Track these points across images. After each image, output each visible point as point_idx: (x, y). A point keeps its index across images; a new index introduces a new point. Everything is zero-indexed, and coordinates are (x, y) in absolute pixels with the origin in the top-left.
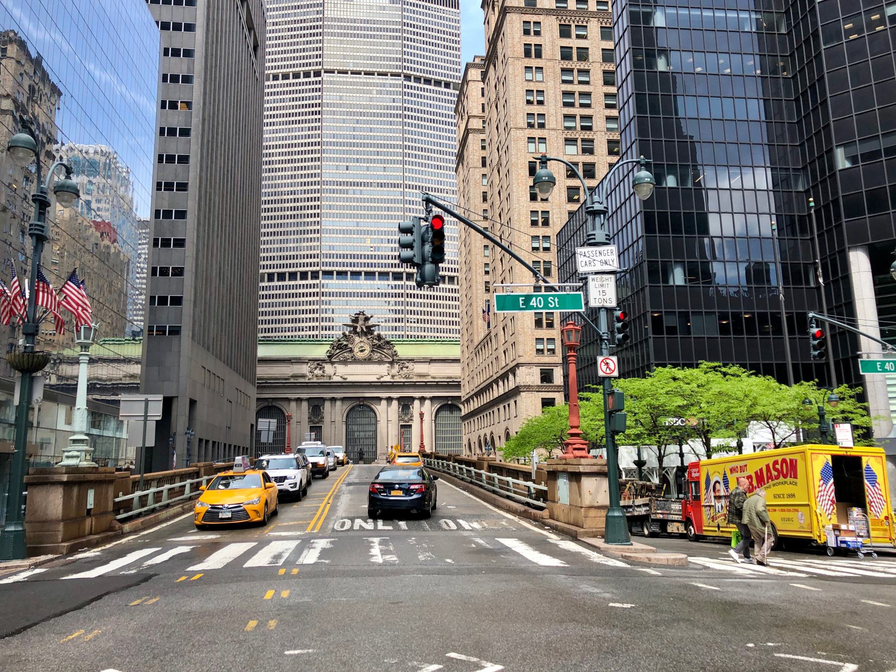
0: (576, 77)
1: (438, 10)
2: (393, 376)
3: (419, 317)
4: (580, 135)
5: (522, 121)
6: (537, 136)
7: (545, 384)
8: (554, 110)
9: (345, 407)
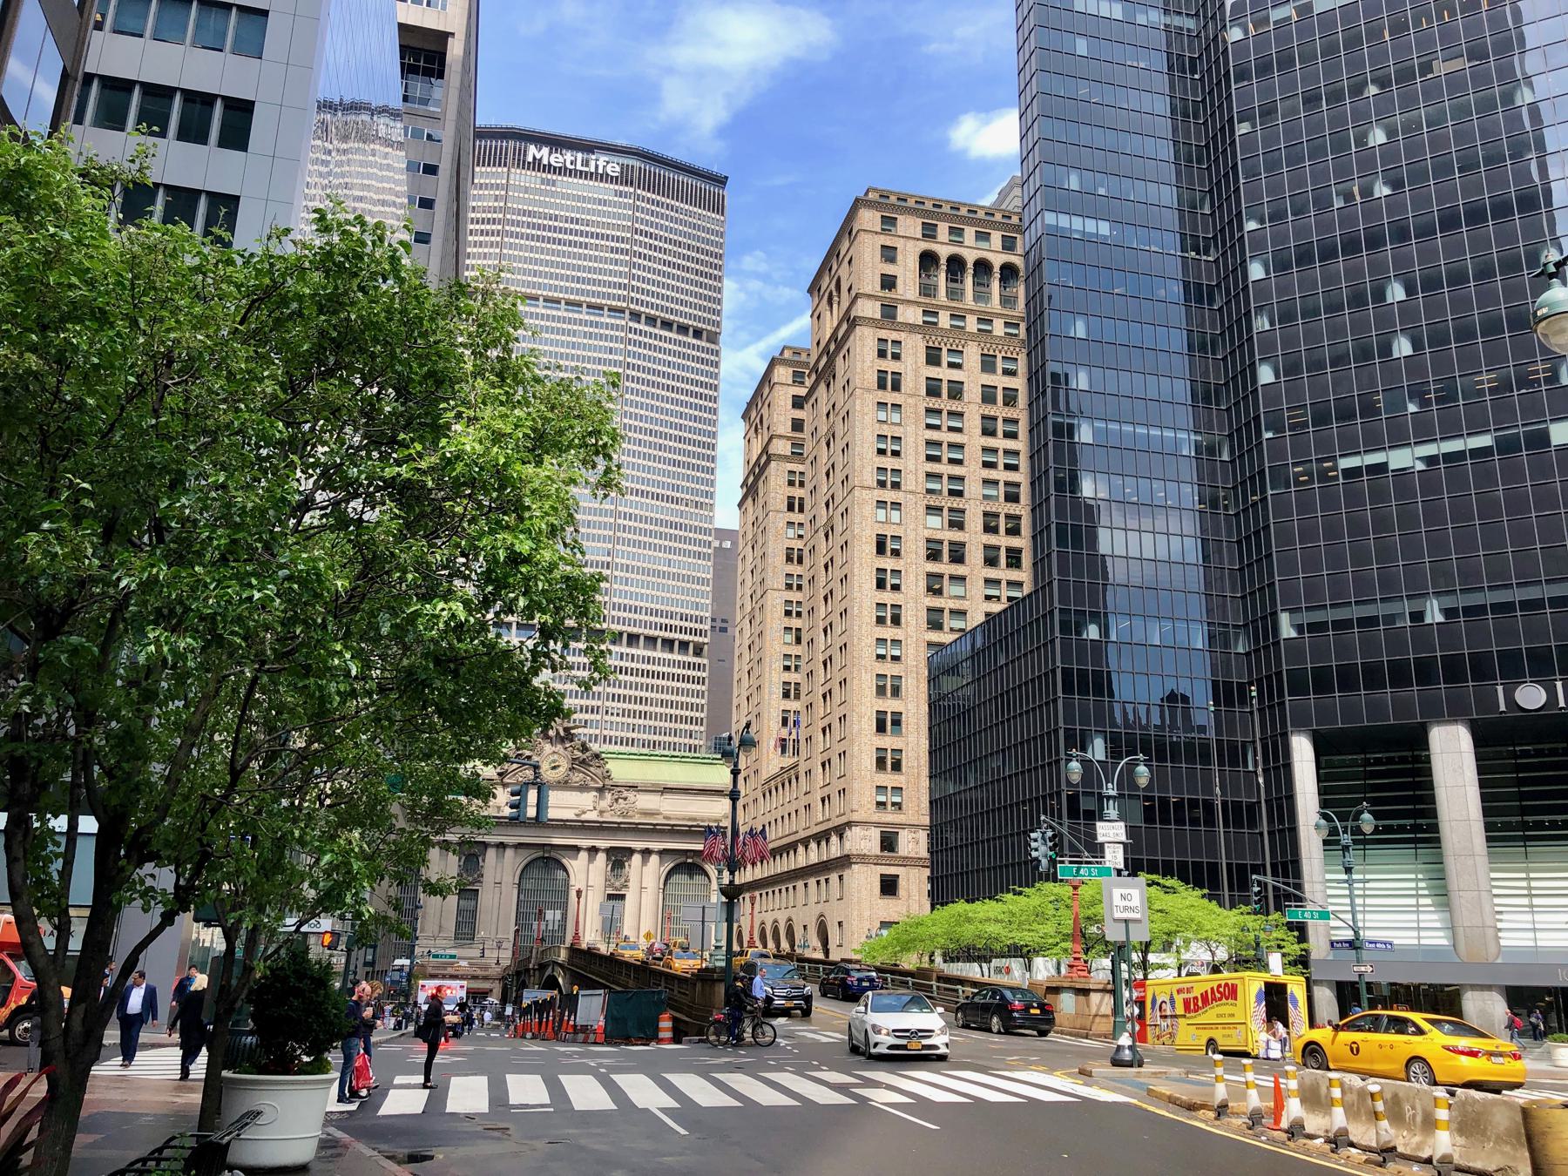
0: (946, 422)
1: (690, 214)
2: (601, 812)
3: (625, 706)
4: (948, 502)
5: (870, 478)
6: (889, 500)
7: (886, 853)
8: (913, 465)
9: (519, 860)
